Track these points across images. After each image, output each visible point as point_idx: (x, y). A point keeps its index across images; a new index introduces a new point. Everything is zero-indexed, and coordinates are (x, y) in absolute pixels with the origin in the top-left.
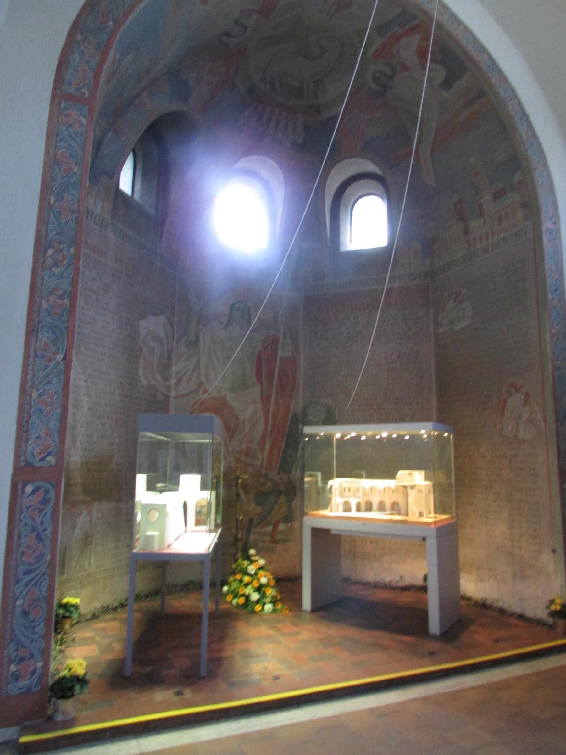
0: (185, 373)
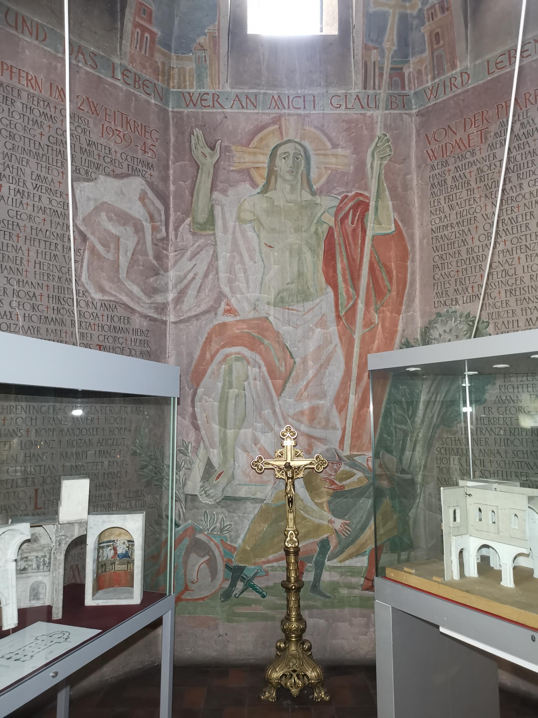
0: (194, 278)
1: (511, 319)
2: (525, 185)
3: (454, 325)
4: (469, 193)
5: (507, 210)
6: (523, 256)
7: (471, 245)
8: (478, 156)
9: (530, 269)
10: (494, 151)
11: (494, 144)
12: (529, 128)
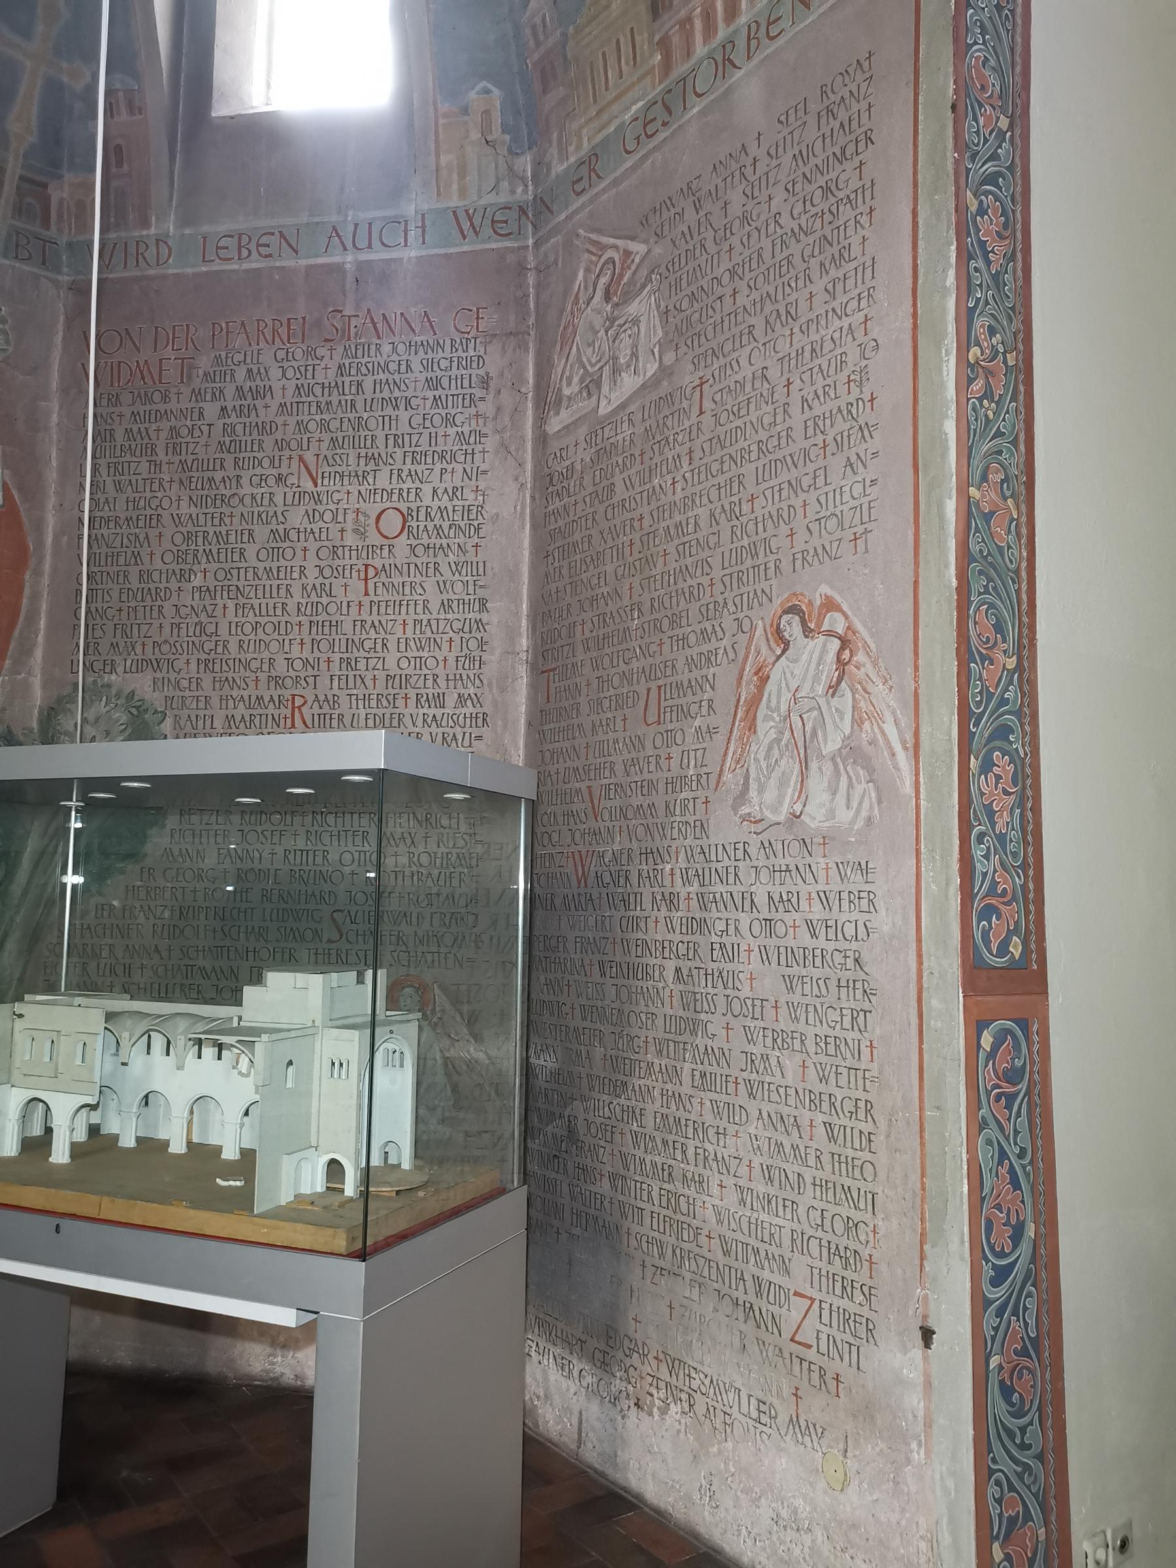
1: (201, 713)
2: (245, 481)
3: (104, 710)
4: (153, 467)
5: (213, 518)
6: (231, 605)
7: (147, 566)
8: (173, 405)
9: (239, 628)
10: (201, 405)
11: (203, 391)
12: (258, 382)
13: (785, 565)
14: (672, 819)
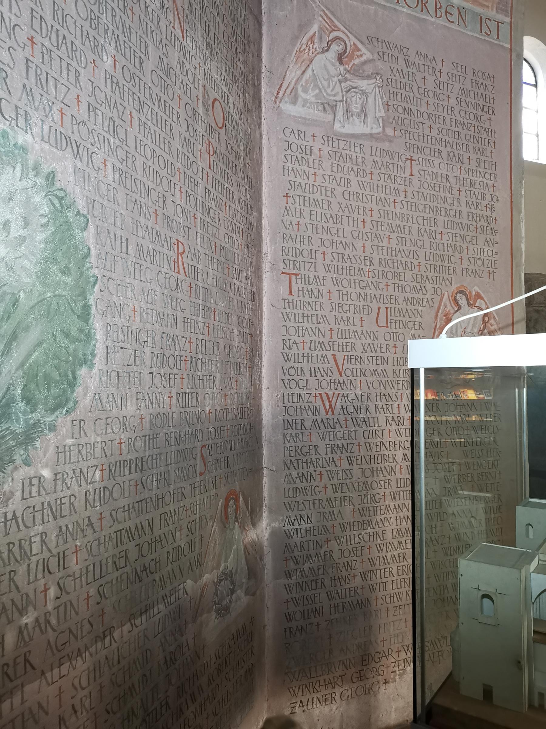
3: (19, 186)
13: (459, 271)
14: (398, 379)
